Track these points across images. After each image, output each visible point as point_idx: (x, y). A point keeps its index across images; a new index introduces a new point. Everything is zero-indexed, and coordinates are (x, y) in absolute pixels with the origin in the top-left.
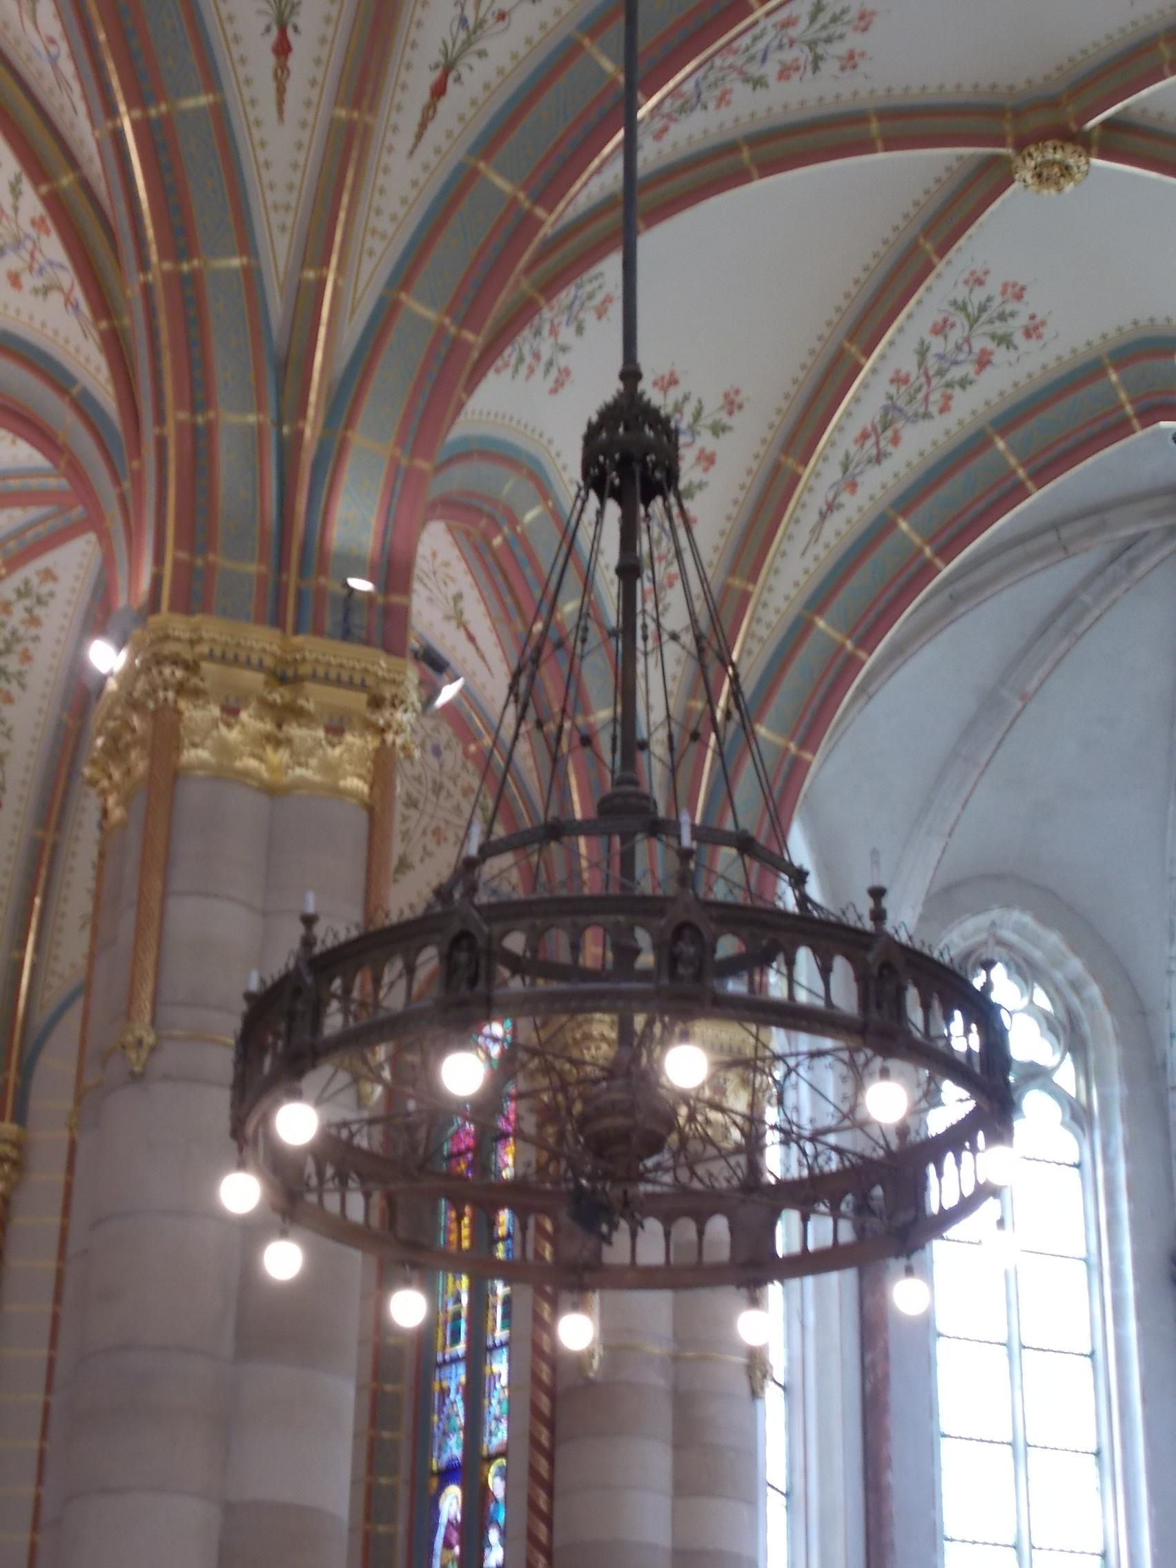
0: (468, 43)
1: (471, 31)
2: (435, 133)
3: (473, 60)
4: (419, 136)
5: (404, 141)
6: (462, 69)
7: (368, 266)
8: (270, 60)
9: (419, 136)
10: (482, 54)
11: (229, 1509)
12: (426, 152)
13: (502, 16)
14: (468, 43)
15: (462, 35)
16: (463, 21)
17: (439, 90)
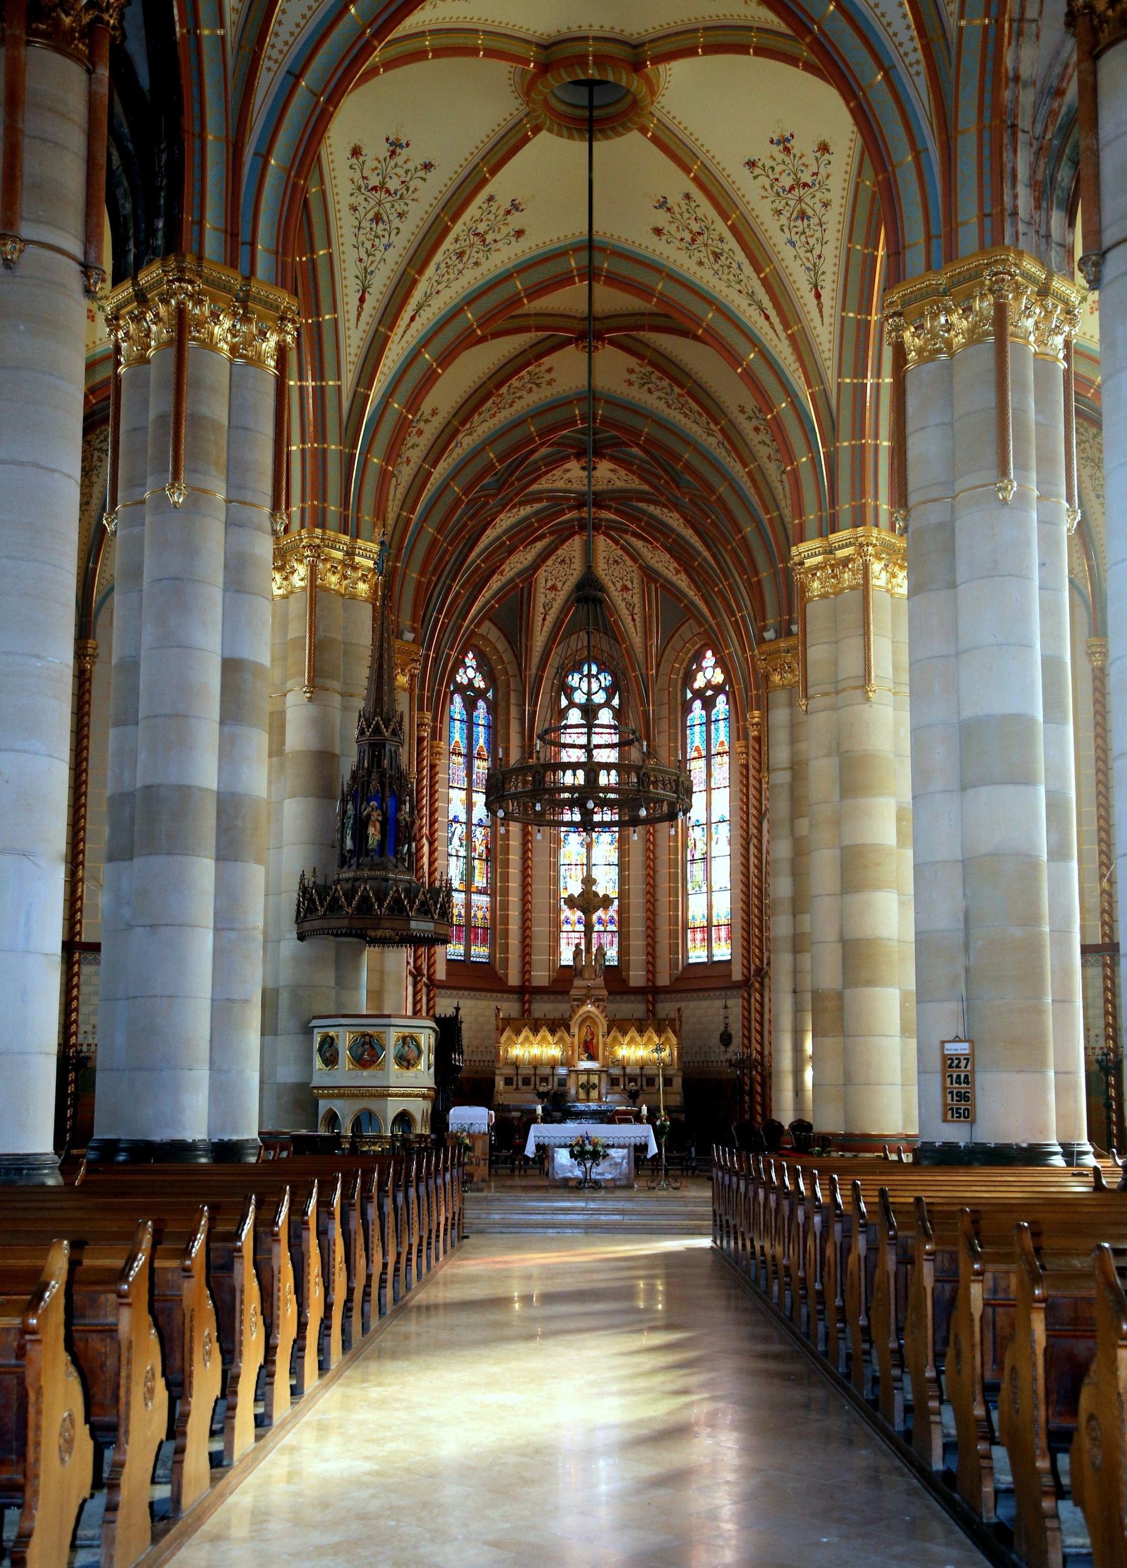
0: (816, 274)
1: (814, 269)
2: (827, 311)
3: (822, 277)
4: (822, 316)
5: (817, 321)
6: (820, 283)
7: (829, 372)
8: (767, 323)
9: (822, 316)
10: (823, 273)
11: (843, 849)
12: (827, 320)
13: (820, 257)
14: (816, 274)
15: (812, 273)
16: (808, 269)
17: (818, 296)
